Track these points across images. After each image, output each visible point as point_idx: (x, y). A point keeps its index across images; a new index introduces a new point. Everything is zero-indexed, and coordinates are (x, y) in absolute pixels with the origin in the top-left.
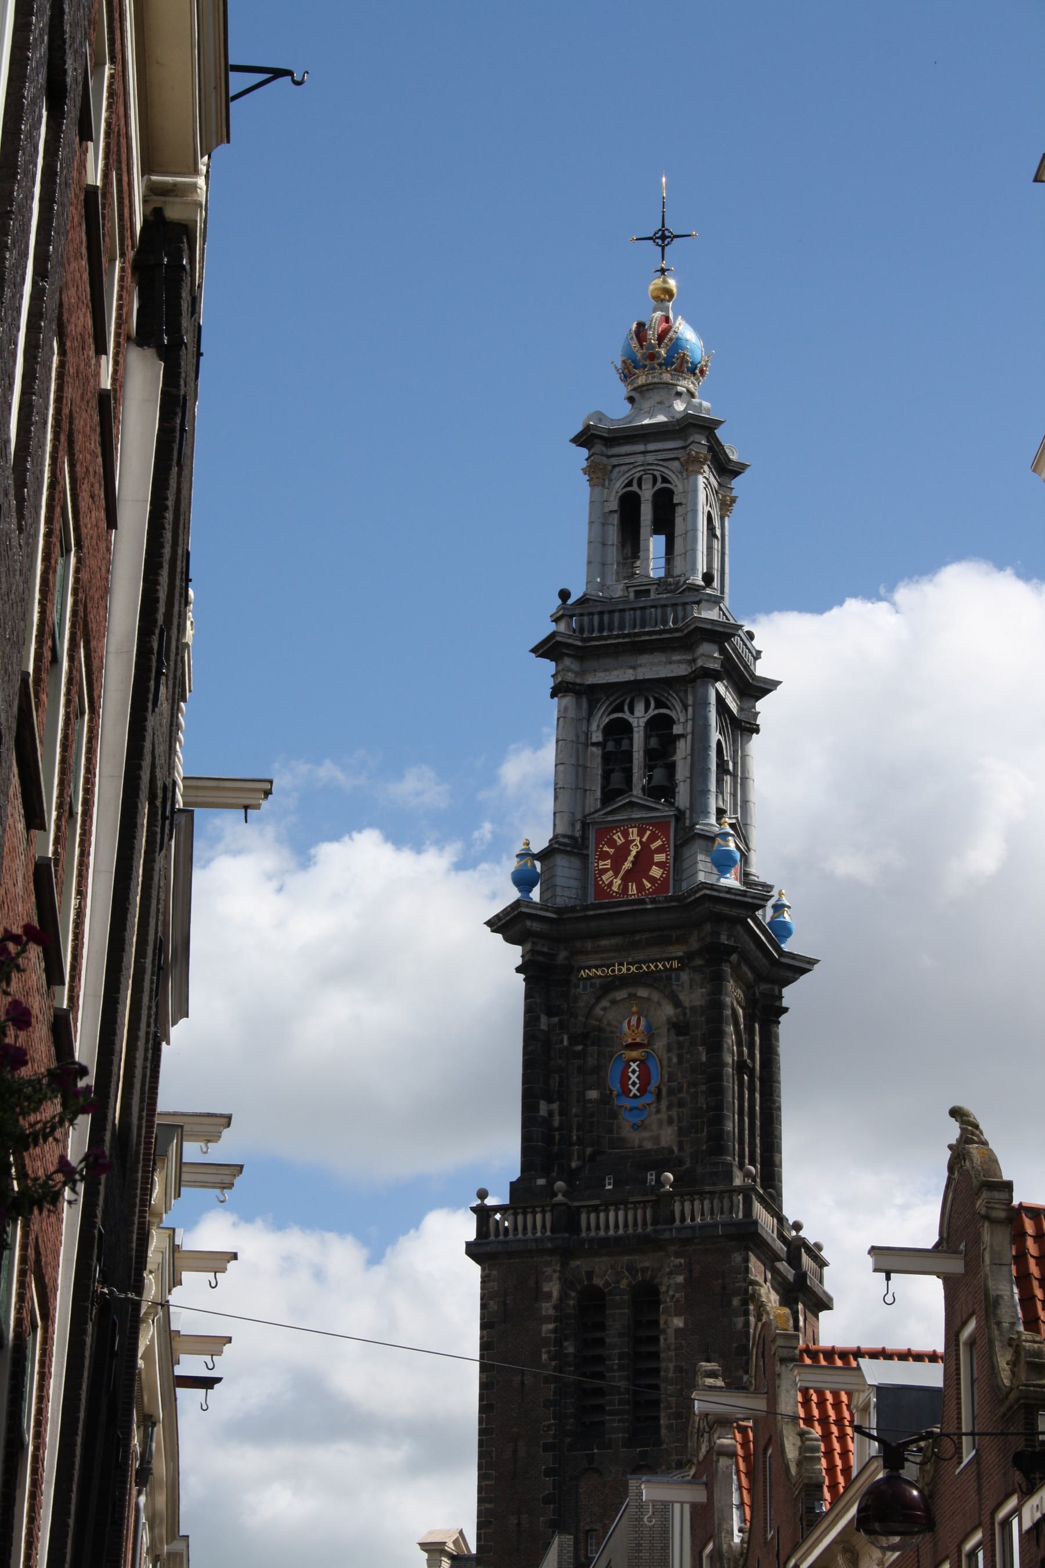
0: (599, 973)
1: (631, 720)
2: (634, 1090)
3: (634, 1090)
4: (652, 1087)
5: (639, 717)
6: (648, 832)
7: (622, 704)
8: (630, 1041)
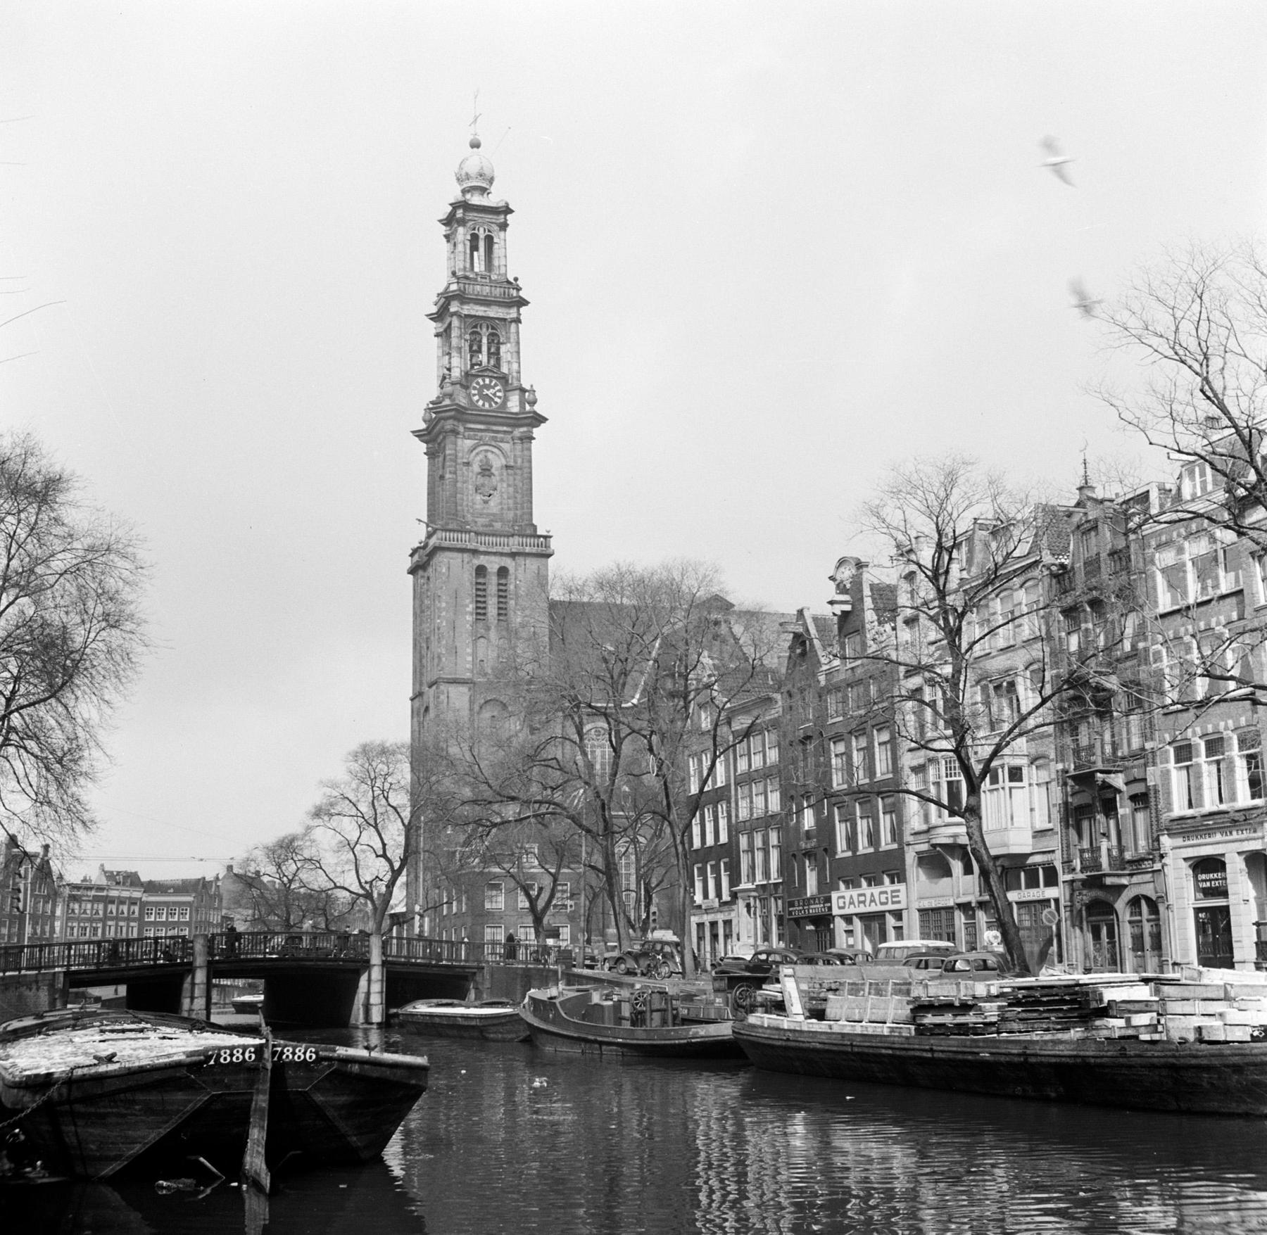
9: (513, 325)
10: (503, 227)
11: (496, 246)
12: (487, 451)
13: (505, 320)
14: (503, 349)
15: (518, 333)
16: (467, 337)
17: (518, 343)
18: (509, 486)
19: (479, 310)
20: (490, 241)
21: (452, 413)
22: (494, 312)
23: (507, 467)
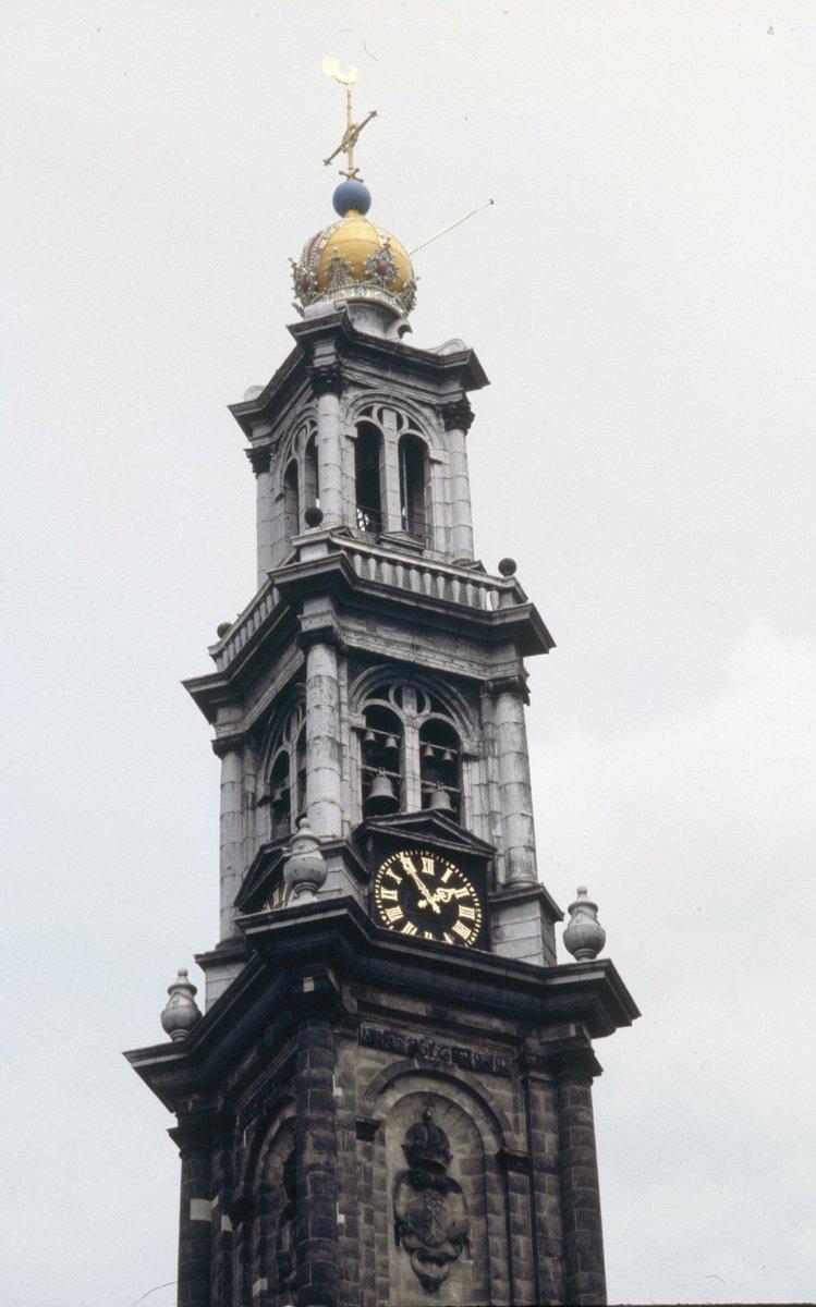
1: (399, 713)
5: (411, 715)
7: (388, 687)
10: (458, 418)
11: (435, 472)
12: (431, 1099)
13: (471, 687)
14: (471, 775)
15: (521, 725)
16: (361, 722)
17: (523, 756)
18: (511, 1228)
19: (394, 645)
20: (415, 456)
21: (320, 938)
22: (436, 658)
23: (505, 1160)
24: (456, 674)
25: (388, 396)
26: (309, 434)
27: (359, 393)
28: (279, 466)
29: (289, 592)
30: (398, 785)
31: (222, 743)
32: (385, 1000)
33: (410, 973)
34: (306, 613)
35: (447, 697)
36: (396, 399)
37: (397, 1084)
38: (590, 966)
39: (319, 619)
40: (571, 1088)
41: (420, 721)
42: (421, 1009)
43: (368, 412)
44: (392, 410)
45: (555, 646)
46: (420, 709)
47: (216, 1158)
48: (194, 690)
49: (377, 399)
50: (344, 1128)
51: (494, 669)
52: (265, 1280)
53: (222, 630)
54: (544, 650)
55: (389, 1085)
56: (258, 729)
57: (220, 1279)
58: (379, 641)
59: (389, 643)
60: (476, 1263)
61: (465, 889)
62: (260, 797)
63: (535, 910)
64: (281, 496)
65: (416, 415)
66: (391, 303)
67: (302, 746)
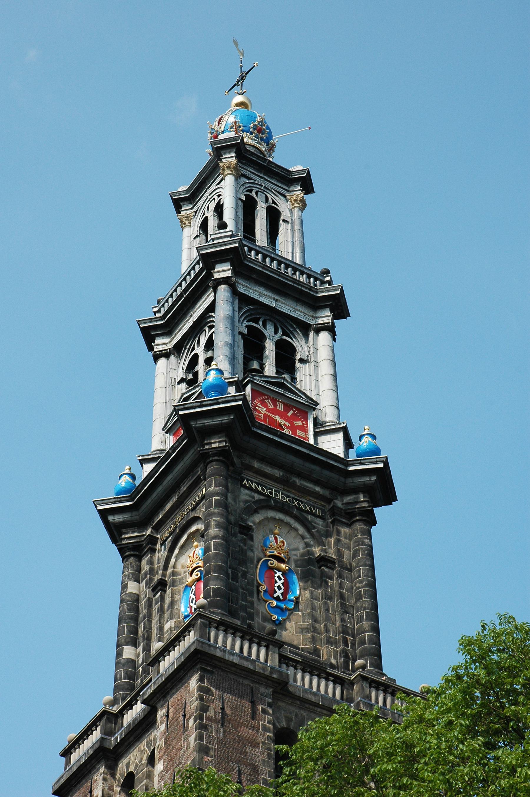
0: (260, 489)
2: (279, 593)
3: (279, 593)
4: (291, 596)
6: (291, 412)
7: (259, 318)
8: (276, 553)
9: (324, 337)
21: (225, 419)
22: (286, 307)
24: (297, 318)
25: (262, 186)
26: (217, 201)
27: (247, 181)
28: (198, 221)
29: (209, 260)
30: (262, 366)
31: (158, 353)
32: (256, 465)
33: (272, 451)
34: (216, 270)
35: (291, 330)
36: (265, 187)
37: (260, 511)
38: (375, 460)
39: (224, 273)
40: (359, 526)
41: (277, 338)
42: (278, 473)
43: (251, 191)
44: (263, 193)
45: (350, 316)
46: (276, 333)
47: (144, 562)
48: (142, 326)
49: (255, 186)
50: (232, 524)
51: (317, 319)
52: (173, 621)
53: (158, 302)
54: (344, 317)
55: (256, 511)
56: (178, 349)
57: (144, 624)
58: (256, 293)
59: (261, 295)
60: (303, 614)
61: (300, 422)
62: (179, 379)
63: (340, 435)
64: (197, 236)
65: (277, 198)
66: (263, 149)
67: (210, 345)
